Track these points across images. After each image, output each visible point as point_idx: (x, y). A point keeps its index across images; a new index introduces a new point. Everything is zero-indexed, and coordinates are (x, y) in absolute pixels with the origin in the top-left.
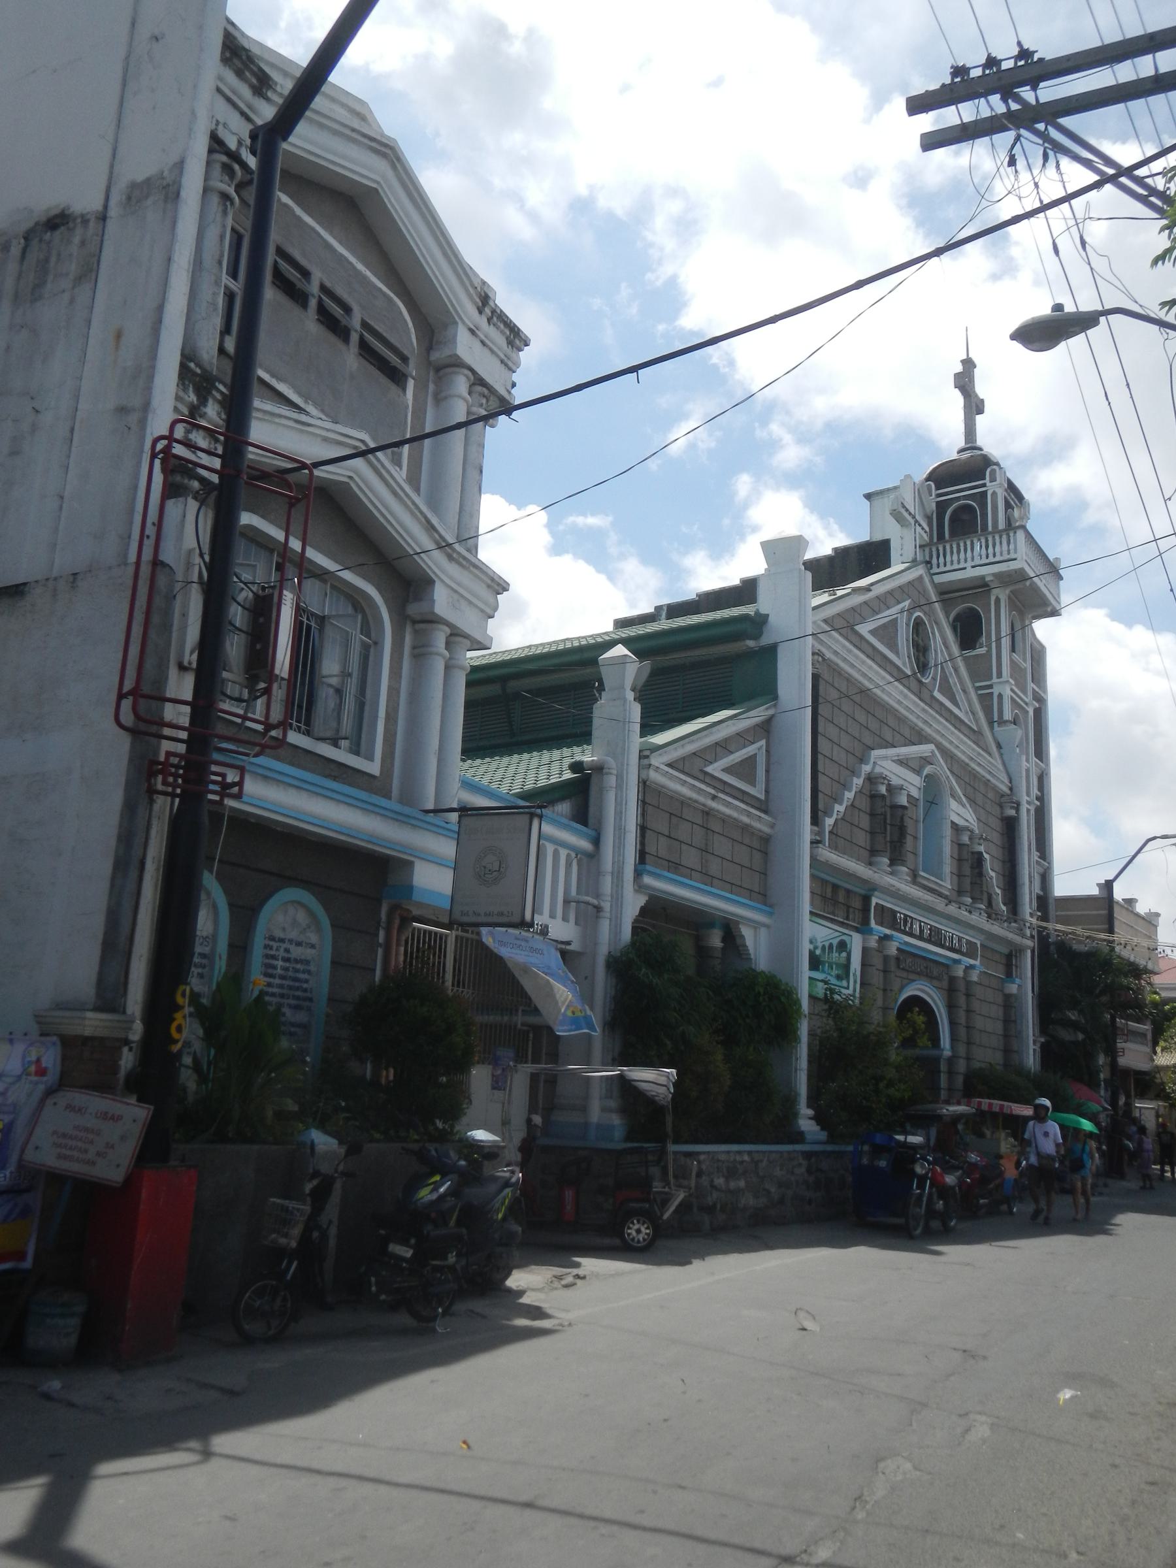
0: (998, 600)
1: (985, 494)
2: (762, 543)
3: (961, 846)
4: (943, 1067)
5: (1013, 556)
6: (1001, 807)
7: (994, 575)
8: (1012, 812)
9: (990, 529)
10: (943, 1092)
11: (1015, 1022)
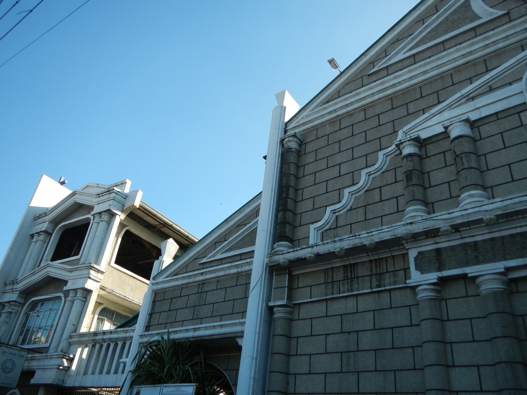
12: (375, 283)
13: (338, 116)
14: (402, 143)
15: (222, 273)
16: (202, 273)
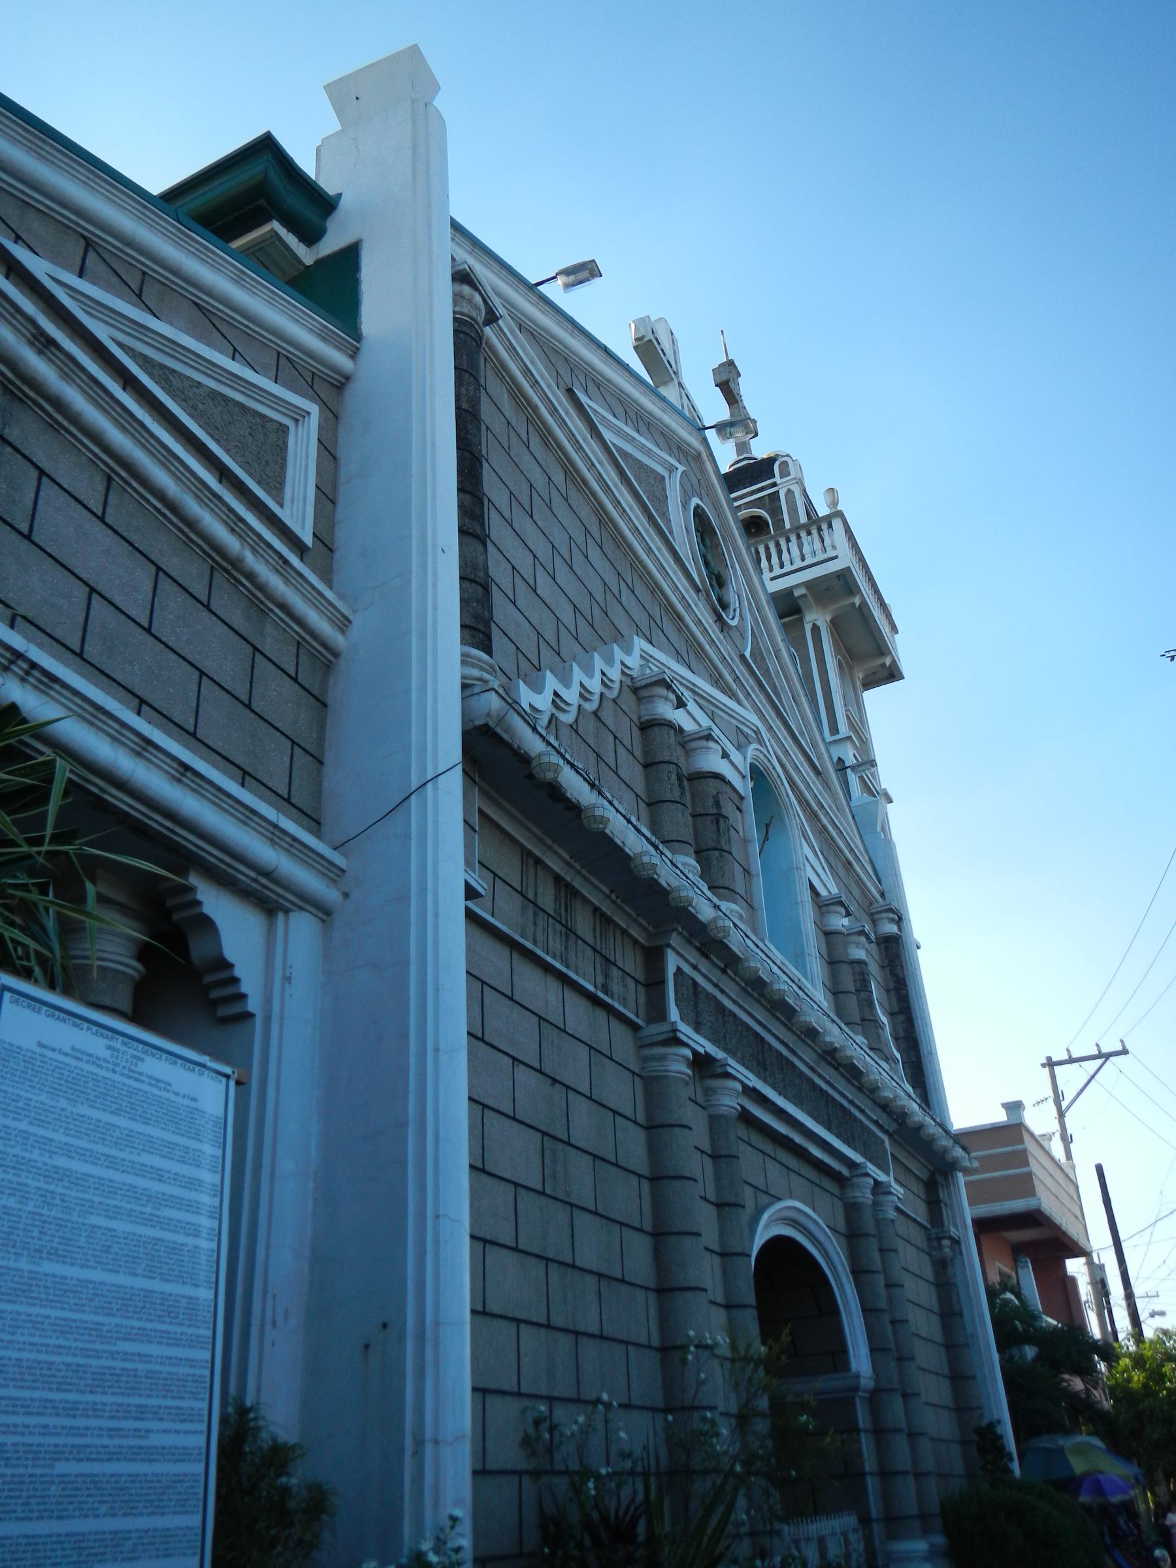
0: (815, 629)
1: (775, 497)
2: (327, 88)
3: (829, 935)
4: (863, 1419)
5: (830, 554)
6: (874, 922)
7: (808, 584)
8: (893, 929)
9: (788, 526)
10: (869, 1480)
11: (961, 1314)
12: (600, 979)
13: (535, 408)
14: (669, 687)
15: (162, 477)
16: (51, 342)
